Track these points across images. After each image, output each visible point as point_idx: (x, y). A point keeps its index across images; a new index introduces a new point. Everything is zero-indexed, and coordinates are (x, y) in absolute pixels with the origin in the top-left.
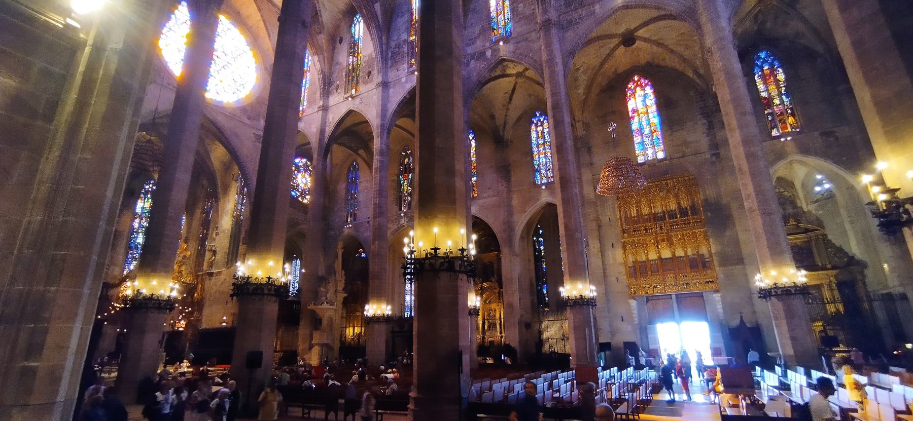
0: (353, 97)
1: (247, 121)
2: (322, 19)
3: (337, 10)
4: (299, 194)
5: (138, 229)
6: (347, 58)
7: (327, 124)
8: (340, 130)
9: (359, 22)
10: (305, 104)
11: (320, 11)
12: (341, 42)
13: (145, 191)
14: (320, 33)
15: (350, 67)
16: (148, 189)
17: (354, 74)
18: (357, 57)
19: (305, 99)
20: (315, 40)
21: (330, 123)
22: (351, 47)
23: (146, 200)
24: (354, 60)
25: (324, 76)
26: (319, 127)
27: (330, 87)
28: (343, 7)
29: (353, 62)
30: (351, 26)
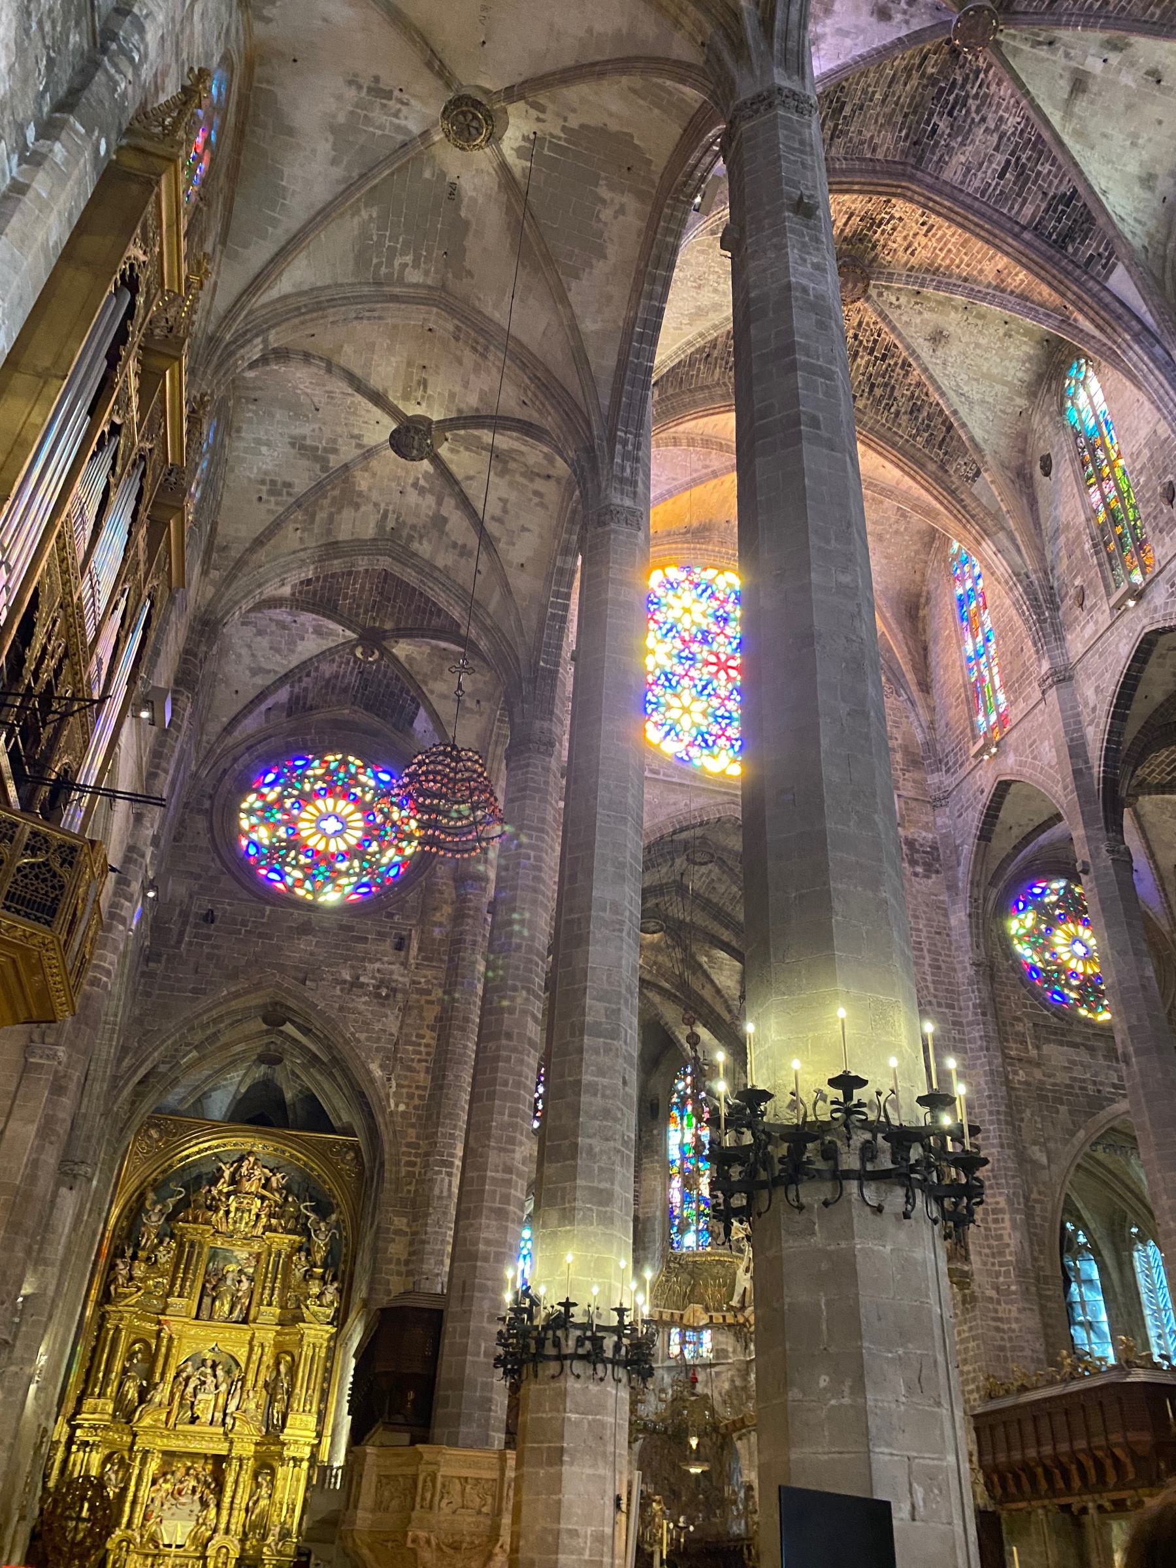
0: (1138, 595)
2: (968, 432)
3: (1006, 390)
4: (1073, 995)
6: (1081, 496)
7: (1086, 718)
8: (1132, 729)
9: (1083, 383)
10: (1001, 697)
11: (955, 412)
12: (1047, 466)
13: (679, 1097)
14: (978, 473)
15: (1102, 517)
17: (1119, 530)
18: (1112, 477)
19: (997, 683)
20: (968, 501)
21: (1094, 709)
22: (1084, 464)
24: (1106, 491)
25: (1029, 589)
26: (1063, 739)
27: (1058, 608)
29: (1104, 497)
30: (1062, 410)
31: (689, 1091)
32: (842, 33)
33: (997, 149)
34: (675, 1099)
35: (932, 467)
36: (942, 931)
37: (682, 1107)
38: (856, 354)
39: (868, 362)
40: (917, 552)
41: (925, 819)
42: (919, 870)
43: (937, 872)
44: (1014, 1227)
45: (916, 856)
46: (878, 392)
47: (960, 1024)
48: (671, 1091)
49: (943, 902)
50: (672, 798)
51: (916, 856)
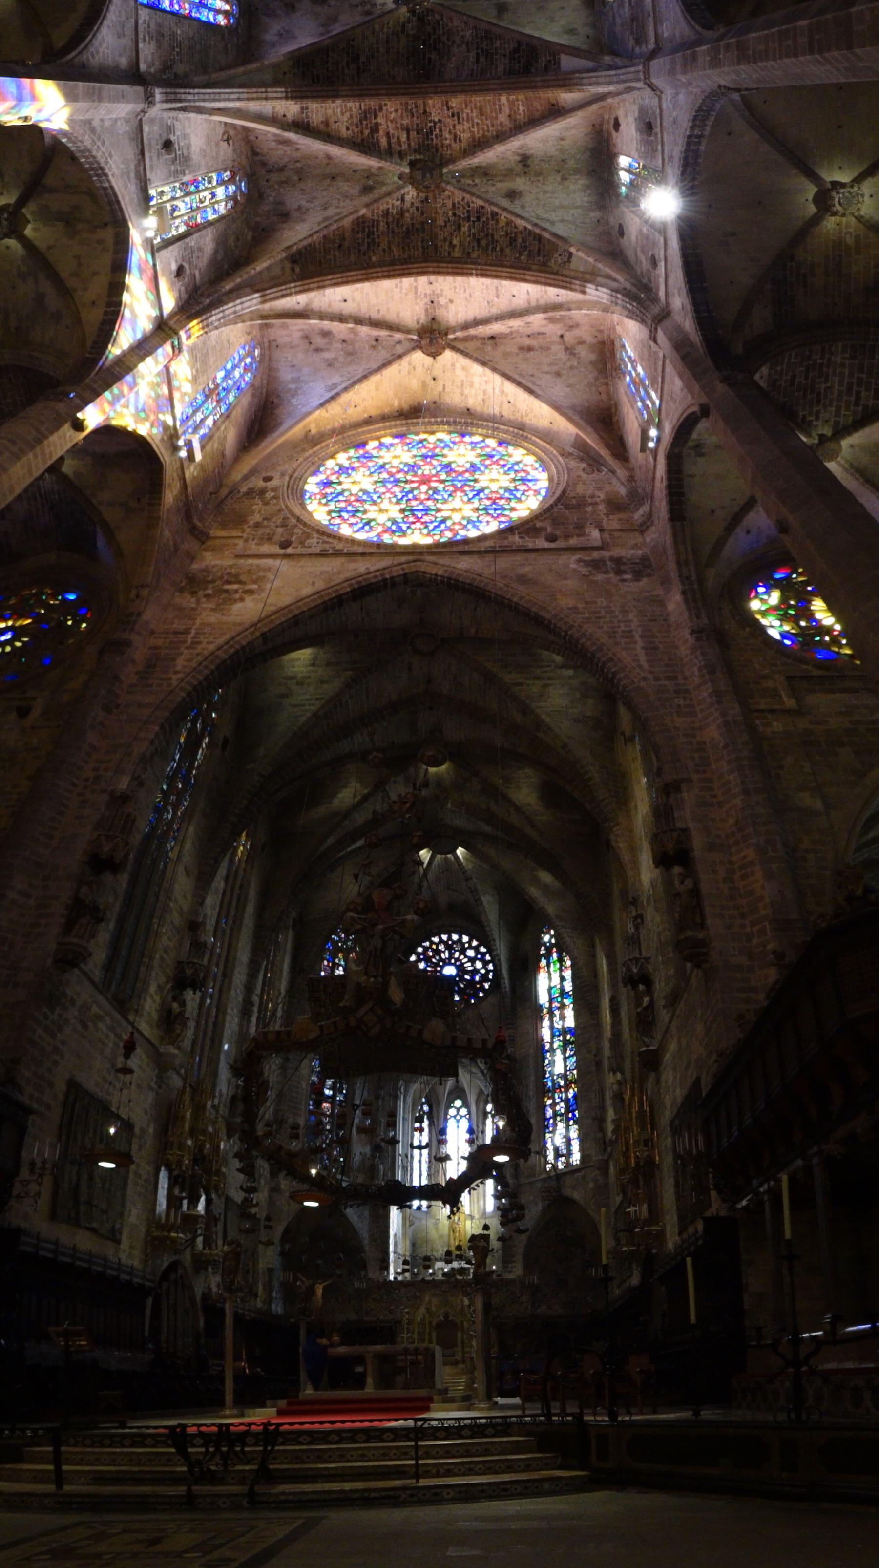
16: (550, 941)
28: (586, 199)
31: (553, 941)
34: (543, 952)
37: (548, 956)
40: (596, 379)
43: (649, 575)
45: (622, 568)
48: (539, 943)
51: (622, 568)
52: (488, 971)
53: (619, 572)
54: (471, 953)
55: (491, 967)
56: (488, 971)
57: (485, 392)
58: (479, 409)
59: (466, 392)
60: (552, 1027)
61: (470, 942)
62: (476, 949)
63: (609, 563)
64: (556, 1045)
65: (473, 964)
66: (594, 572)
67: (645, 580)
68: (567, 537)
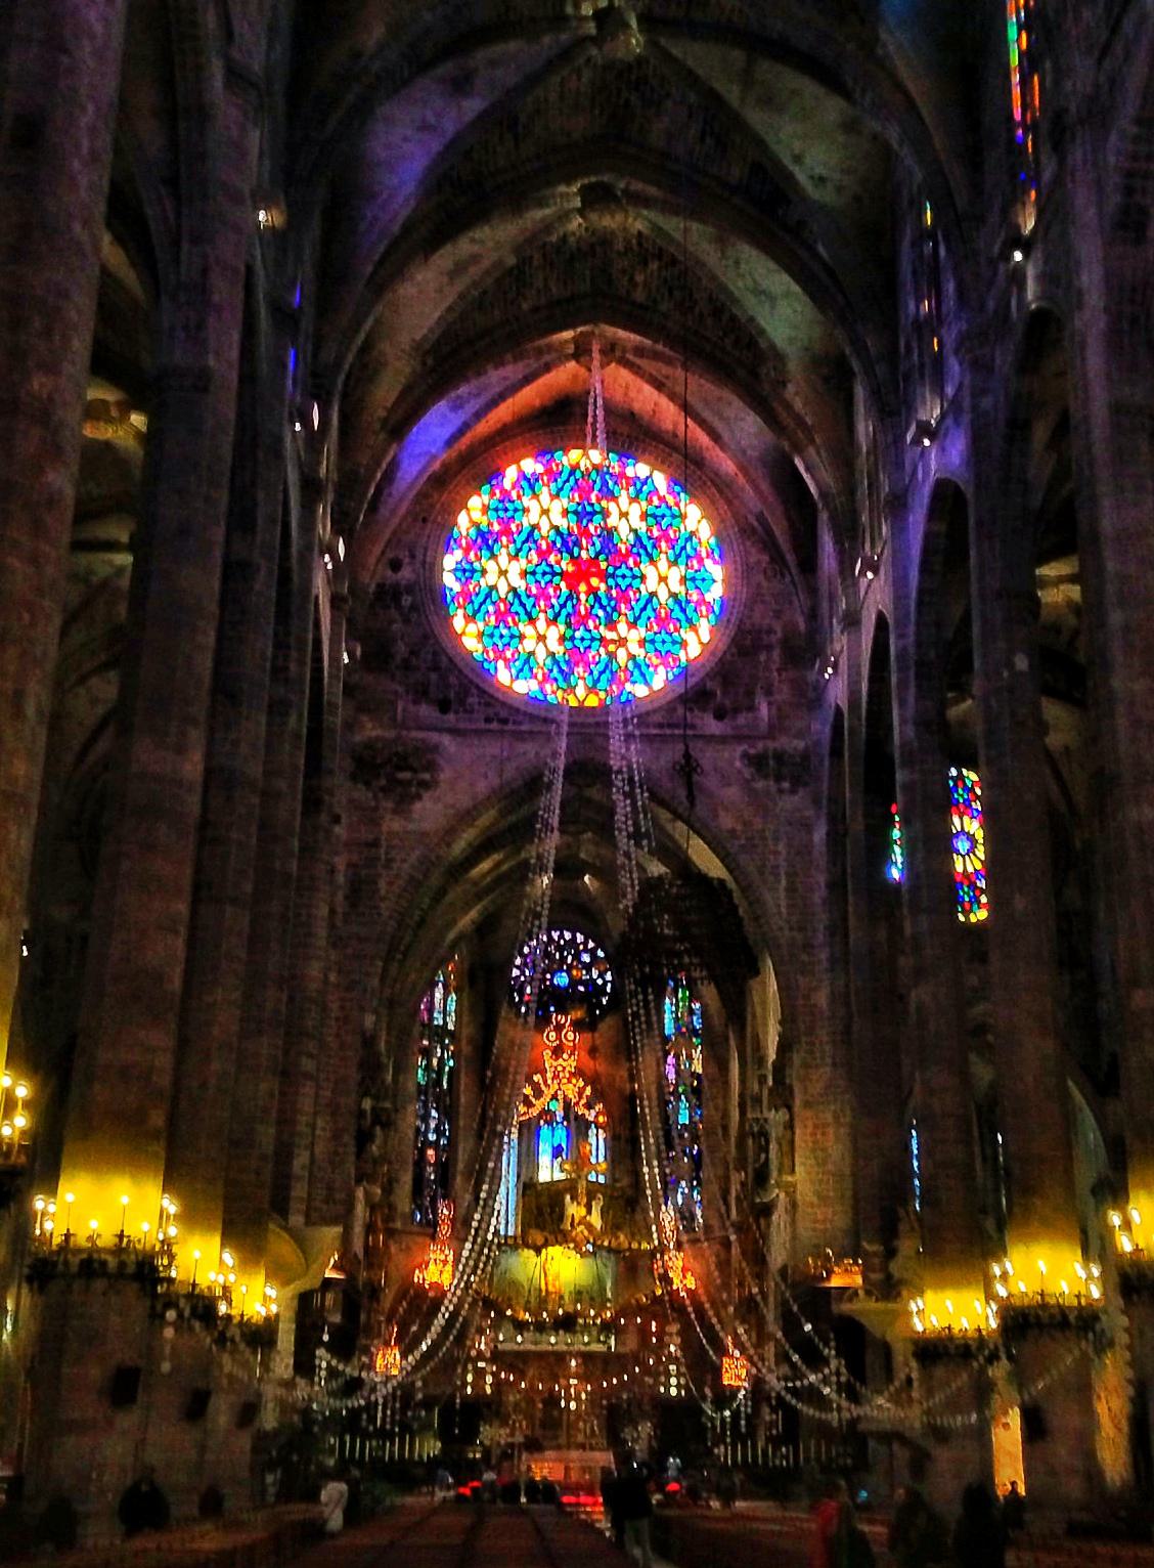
1: (713, 726)
5: (676, 1086)
23: (680, 995)
32: (493, 63)
33: (690, 116)
35: (741, 373)
36: (806, 850)
38: (646, 264)
39: (660, 268)
41: (799, 724)
42: (786, 785)
43: (806, 784)
44: (837, 1139)
45: (785, 770)
46: (677, 293)
47: (813, 947)
49: (808, 818)
50: (521, 747)
51: (785, 770)
52: (605, 983)
53: (779, 778)
54: (586, 958)
55: (609, 977)
56: (605, 983)
57: (655, 404)
58: (646, 418)
59: (632, 394)
60: (677, 1066)
61: (585, 943)
62: (593, 953)
63: (771, 762)
64: (681, 1090)
65: (589, 972)
66: (757, 777)
67: (801, 792)
68: (736, 711)
